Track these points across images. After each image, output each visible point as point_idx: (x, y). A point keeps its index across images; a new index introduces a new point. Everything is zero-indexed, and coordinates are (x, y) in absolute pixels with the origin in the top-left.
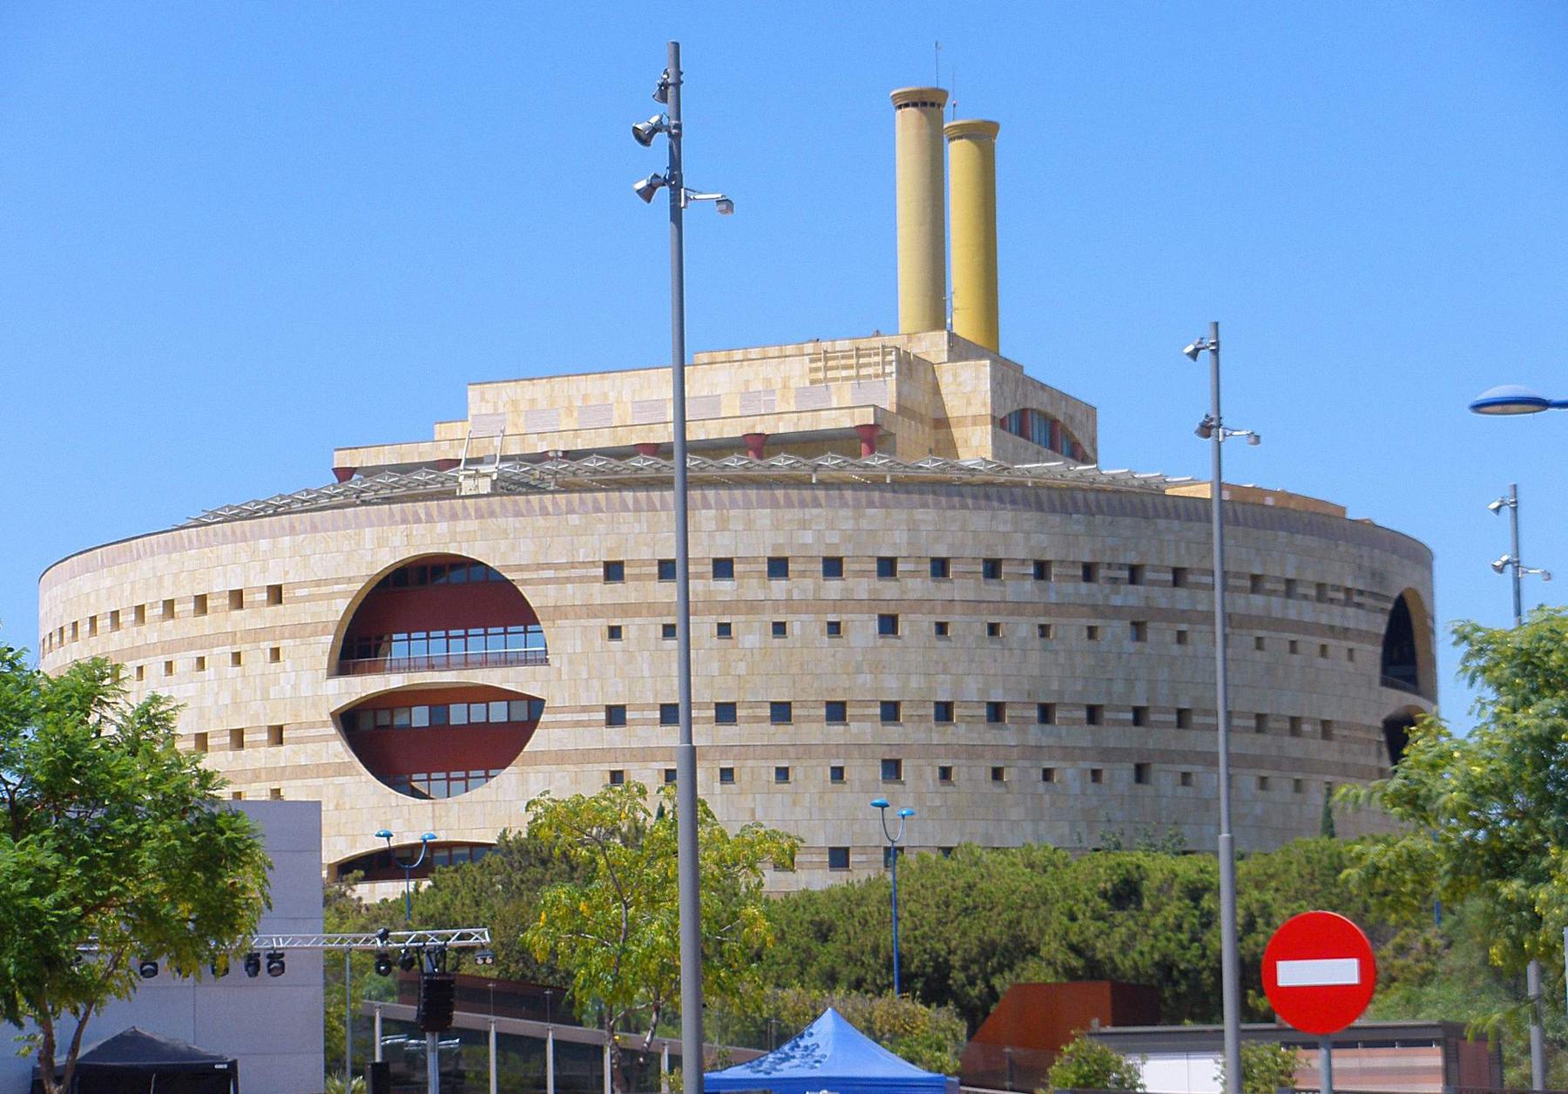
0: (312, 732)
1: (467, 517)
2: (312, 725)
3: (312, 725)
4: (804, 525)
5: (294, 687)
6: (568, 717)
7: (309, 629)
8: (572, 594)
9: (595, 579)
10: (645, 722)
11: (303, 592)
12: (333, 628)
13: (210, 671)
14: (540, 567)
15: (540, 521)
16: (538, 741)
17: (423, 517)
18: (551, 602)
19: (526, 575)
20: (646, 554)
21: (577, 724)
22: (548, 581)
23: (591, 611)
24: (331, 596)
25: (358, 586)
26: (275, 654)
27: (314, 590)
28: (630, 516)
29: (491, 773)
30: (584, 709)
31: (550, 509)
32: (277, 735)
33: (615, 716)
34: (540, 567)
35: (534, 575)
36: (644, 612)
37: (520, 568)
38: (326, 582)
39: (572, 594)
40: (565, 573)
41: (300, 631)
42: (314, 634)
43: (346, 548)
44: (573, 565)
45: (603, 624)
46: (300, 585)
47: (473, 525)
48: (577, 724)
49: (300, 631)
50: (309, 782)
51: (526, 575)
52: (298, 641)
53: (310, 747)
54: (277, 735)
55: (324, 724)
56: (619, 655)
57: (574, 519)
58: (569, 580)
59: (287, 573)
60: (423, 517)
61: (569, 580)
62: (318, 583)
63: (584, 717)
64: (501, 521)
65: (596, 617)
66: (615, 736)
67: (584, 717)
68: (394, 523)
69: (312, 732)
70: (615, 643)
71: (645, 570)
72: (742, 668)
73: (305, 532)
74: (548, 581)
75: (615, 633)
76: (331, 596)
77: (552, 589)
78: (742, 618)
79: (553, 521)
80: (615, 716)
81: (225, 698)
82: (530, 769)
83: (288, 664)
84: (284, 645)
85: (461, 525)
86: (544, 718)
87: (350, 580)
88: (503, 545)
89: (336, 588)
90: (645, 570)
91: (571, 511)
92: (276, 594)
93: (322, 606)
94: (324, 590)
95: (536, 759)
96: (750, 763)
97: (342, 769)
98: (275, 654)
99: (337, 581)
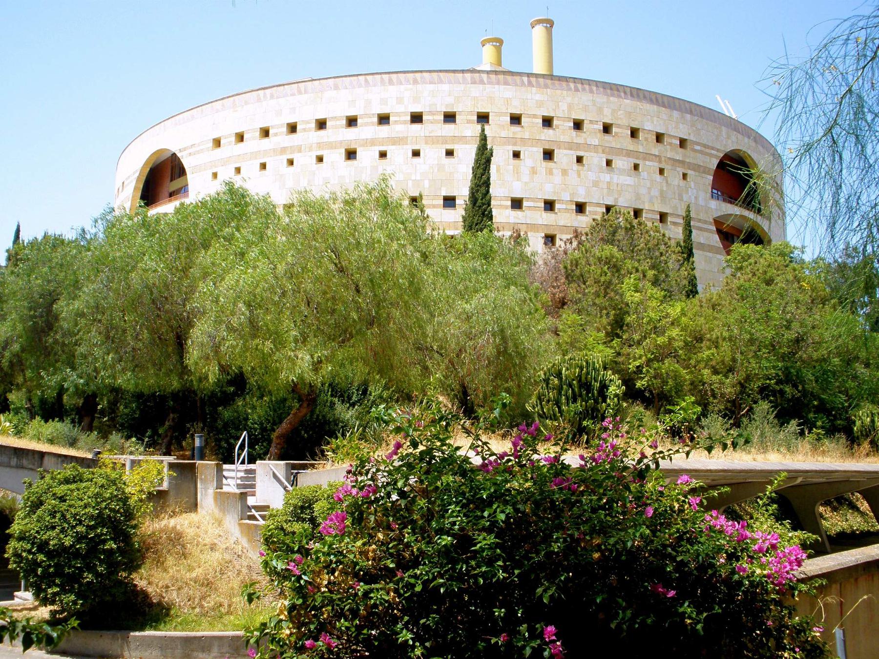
2: (705, 222)
3: (705, 222)
11: (698, 148)
24: (711, 155)
27: (703, 149)
42: (704, 172)
46: (698, 144)
49: (697, 168)
52: (697, 174)
53: (706, 234)
62: (705, 146)
76: (711, 155)
83: (692, 184)
87: (718, 150)
89: (713, 152)
92: (683, 143)
93: (708, 159)
94: (707, 150)
98: (685, 176)
99: (713, 148)
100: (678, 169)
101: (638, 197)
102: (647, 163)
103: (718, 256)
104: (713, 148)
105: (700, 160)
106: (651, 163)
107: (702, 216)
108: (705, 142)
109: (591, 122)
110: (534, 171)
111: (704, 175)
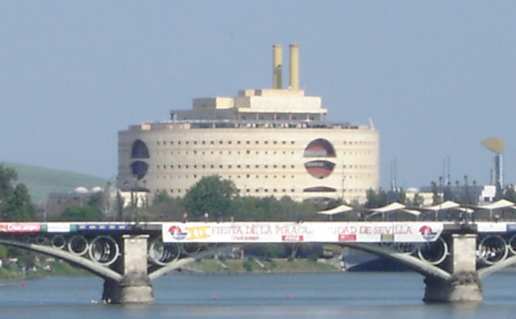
13: (277, 155)
26: (293, 153)
54: (293, 167)
84: (295, 152)
98: (293, 153)
110: (243, 157)
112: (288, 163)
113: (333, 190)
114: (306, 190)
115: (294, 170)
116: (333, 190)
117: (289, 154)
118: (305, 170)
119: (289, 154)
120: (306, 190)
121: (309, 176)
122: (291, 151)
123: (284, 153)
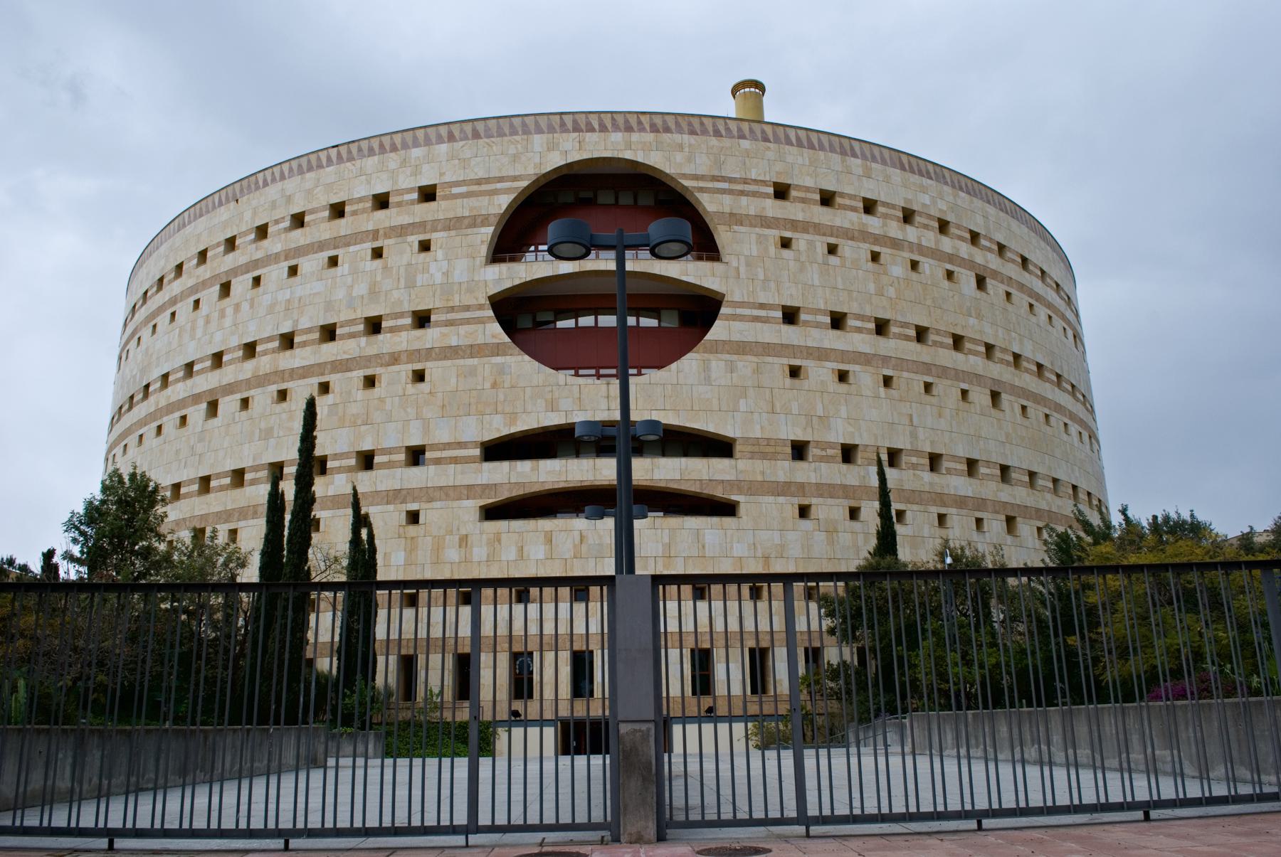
0: (467, 315)
1: (642, 130)
2: (467, 308)
3: (467, 308)
4: (924, 190)
5: (446, 274)
6: (747, 312)
7: (466, 222)
8: (748, 206)
9: (766, 196)
10: (818, 325)
12: (494, 220)
14: (715, 178)
15: (714, 141)
16: (718, 331)
17: (597, 127)
18: (727, 210)
19: (701, 184)
20: (809, 182)
21: (756, 319)
22: (724, 191)
23: (765, 222)
25: (525, 184)
26: (425, 246)
27: (475, 188)
28: (794, 150)
29: (643, 371)
30: (762, 306)
31: (723, 133)
32: (422, 320)
33: (790, 316)
34: (715, 178)
35: (710, 185)
36: (811, 230)
37: (696, 177)
38: (488, 180)
39: (748, 206)
40: (741, 186)
41: (454, 224)
42: (473, 225)
43: (512, 150)
44: (745, 181)
45: (774, 234)
47: (649, 137)
48: (756, 319)
49: (454, 224)
50: (461, 362)
51: (701, 184)
52: (453, 233)
53: (463, 329)
54: (422, 320)
55: (481, 307)
56: (792, 264)
57: (745, 144)
58: (742, 193)
59: (442, 174)
60: (597, 127)
61: (742, 193)
62: (479, 182)
63: (762, 313)
64: (677, 137)
65: (769, 227)
66: (790, 334)
67: (762, 313)
68: (567, 131)
69: (467, 315)
70: (786, 252)
71: (810, 196)
72: (891, 292)
73: (466, 138)
74: (724, 191)
75: (786, 243)
77: (727, 199)
78: (888, 251)
79: (726, 142)
80: (790, 316)
81: (361, 289)
82: (711, 356)
84: (436, 237)
85: (635, 137)
86: (723, 310)
87: (515, 178)
88: (679, 157)
89: (499, 186)
90: (810, 196)
91: (742, 137)
92: (428, 194)
93: (484, 201)
94: (484, 187)
95: (718, 347)
96: (905, 374)
97: (497, 350)
98: (425, 246)
99: (501, 179)
100: (410, 239)
101: (329, 306)
102: (352, 249)
103: (499, 360)
104: (501, 179)
105: (463, 208)
106: (357, 247)
107: (456, 302)
108: (481, 174)
109: (277, 222)
111: (469, 231)
112: (396, 301)
113: (719, 447)
114: (497, 450)
115: (430, 337)
116: (719, 447)
117: (402, 253)
118: (495, 331)
119: (402, 253)
120: (497, 450)
121: (522, 365)
122: (414, 240)
123: (377, 253)
